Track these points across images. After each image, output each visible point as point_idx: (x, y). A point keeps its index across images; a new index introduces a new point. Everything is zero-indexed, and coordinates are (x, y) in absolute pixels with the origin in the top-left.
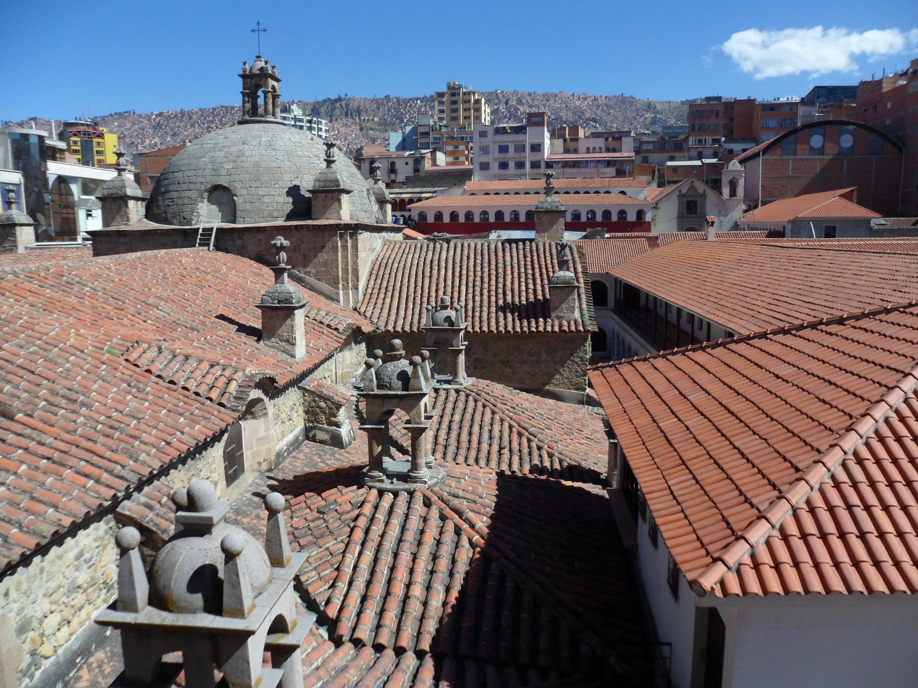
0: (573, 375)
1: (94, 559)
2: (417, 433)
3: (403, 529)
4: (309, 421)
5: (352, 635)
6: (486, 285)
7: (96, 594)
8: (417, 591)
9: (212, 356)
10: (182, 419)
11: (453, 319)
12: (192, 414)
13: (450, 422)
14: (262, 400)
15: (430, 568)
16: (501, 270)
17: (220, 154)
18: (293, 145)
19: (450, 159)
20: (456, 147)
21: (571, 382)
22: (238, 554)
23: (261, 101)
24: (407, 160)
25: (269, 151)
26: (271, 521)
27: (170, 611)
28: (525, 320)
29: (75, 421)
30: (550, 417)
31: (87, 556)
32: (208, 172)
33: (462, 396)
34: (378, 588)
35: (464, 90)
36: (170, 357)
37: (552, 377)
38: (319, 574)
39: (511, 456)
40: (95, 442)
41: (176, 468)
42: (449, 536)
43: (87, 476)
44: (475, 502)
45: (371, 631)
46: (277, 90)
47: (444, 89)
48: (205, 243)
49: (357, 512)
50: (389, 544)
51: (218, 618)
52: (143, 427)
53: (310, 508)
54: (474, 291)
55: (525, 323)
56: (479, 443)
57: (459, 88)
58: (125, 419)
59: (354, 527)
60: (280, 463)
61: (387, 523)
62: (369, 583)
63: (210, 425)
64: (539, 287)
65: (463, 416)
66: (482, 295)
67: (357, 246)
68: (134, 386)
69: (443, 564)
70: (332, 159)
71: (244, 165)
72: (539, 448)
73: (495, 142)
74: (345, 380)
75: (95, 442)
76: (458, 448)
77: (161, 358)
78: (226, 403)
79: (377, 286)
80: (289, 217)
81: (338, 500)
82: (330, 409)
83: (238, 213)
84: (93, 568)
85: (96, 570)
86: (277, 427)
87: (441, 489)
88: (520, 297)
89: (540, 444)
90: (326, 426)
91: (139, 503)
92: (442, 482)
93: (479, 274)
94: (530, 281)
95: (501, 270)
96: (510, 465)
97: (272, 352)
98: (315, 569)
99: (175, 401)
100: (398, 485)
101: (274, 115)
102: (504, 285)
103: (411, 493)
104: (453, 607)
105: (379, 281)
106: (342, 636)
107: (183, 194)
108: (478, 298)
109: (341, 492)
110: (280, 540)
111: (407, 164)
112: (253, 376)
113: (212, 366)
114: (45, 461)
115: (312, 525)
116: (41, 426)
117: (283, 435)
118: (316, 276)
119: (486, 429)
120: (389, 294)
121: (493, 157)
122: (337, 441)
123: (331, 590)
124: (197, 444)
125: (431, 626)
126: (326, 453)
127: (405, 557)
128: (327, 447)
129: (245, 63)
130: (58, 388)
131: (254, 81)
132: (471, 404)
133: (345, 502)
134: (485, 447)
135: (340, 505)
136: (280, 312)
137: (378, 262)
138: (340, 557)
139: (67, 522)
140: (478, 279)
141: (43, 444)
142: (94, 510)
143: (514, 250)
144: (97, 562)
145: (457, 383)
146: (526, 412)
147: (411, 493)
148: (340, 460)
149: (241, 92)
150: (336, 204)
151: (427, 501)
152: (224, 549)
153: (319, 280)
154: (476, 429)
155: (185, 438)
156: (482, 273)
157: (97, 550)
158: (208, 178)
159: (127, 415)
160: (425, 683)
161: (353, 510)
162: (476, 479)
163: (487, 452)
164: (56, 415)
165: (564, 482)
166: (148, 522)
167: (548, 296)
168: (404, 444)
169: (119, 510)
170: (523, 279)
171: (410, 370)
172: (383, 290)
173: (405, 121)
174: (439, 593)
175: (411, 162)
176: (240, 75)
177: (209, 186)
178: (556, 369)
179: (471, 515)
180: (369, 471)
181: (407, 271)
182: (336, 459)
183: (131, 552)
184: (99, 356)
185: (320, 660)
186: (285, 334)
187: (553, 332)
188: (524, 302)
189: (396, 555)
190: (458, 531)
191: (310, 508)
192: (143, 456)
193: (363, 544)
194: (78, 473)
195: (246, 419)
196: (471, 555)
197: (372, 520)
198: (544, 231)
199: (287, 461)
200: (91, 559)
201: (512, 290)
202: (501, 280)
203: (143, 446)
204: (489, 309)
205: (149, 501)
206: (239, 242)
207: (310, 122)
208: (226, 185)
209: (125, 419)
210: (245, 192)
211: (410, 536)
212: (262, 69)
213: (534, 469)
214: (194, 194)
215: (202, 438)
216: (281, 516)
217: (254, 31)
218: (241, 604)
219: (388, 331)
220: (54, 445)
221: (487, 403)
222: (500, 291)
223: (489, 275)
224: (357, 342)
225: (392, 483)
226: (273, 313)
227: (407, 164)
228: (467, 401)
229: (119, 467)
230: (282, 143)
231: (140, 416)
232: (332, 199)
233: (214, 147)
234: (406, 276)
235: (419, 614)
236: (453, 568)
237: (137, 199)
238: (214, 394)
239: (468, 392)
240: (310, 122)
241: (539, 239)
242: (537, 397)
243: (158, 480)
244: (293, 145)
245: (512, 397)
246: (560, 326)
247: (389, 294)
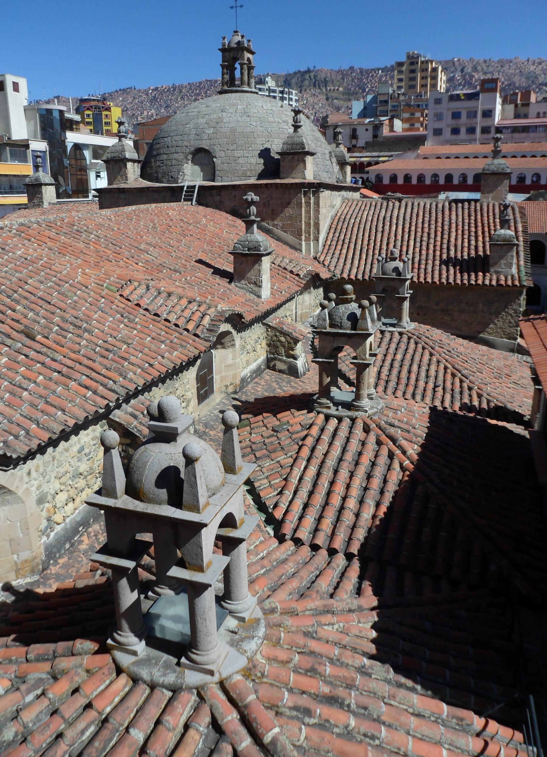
0: (506, 325)
1: (92, 454)
2: (361, 368)
3: (344, 450)
4: (270, 353)
5: (294, 535)
6: (432, 241)
7: (94, 481)
8: (352, 503)
9: (190, 294)
10: (163, 346)
11: (401, 269)
12: (171, 342)
13: (393, 360)
14: (231, 333)
15: (364, 485)
16: (446, 227)
17: (202, 121)
18: (265, 111)
19: (407, 126)
20: (413, 114)
21: (504, 332)
22: (197, 460)
23: (237, 74)
24: (368, 127)
25: (244, 118)
26: (227, 435)
27: (141, 501)
28: (466, 274)
29: (79, 344)
30: (482, 362)
31: (87, 451)
32: (192, 137)
33: (405, 339)
34: (319, 499)
36: (155, 294)
38: (270, 482)
39: (444, 393)
40: (94, 361)
41: (157, 386)
42: (383, 459)
43: (87, 388)
44: (408, 432)
45: (310, 533)
48: (189, 199)
49: (305, 432)
50: (331, 462)
51: (178, 510)
52: (131, 350)
53: (266, 427)
54: (421, 246)
55: (466, 276)
56: (417, 380)
58: (118, 344)
59: (302, 445)
60: (244, 387)
61: (331, 444)
62: (311, 493)
63: (186, 352)
64: (480, 244)
65: (404, 356)
66: (428, 249)
67: (318, 202)
68: (126, 317)
69: (376, 483)
70: (299, 124)
72: (470, 389)
73: (448, 109)
74: (303, 320)
75: (94, 361)
76: (397, 384)
77: (149, 294)
78: (200, 334)
79: (336, 239)
80: (261, 176)
81: (290, 422)
82: (289, 343)
83: (217, 172)
84: (91, 460)
85: (93, 461)
86: (243, 356)
87: (380, 418)
88: (462, 252)
89: (471, 385)
90: (285, 358)
91: (126, 413)
92: (381, 411)
93: (426, 230)
94: (473, 238)
95: (446, 227)
96: (442, 402)
97: (242, 292)
98: (267, 477)
99: (159, 331)
100: (343, 412)
101: (249, 85)
102: (449, 241)
103: (353, 420)
104: (381, 520)
105: (337, 235)
106: (285, 535)
107: (171, 156)
108: (424, 252)
109: (293, 414)
110: (234, 452)
111: (367, 130)
112: (223, 311)
113: (190, 302)
114: (56, 374)
115: (267, 441)
116: (54, 346)
117: (248, 363)
118: (282, 228)
119: (424, 368)
120: (346, 246)
121: (447, 124)
122: (293, 371)
123: (279, 496)
124: (174, 367)
125: (361, 534)
126: (284, 380)
127: (344, 474)
128: (285, 376)
130: (67, 316)
132: (412, 346)
133: (296, 424)
134: (421, 384)
135: (292, 426)
136: (249, 258)
137: (337, 218)
138: (288, 470)
139: (71, 423)
140: (425, 235)
141: (55, 361)
142: (91, 415)
143: (460, 210)
144: (94, 457)
145: (401, 326)
146: (461, 356)
147: (353, 420)
148: (295, 387)
150: (302, 165)
152: (185, 455)
153: (285, 232)
154: (415, 368)
155: (165, 362)
156: (429, 229)
157: (94, 447)
158: (192, 142)
159: (119, 341)
160: (350, 581)
161: (302, 430)
162: (411, 412)
163: (423, 389)
164: (65, 337)
165: (489, 421)
166: (132, 429)
167: (488, 253)
168: (351, 377)
169: (111, 416)
170: (466, 236)
171: (358, 312)
172: (340, 243)
173: (367, 90)
174: (370, 507)
175: (370, 128)
177: (193, 149)
178: (491, 320)
179: (404, 443)
180: (318, 398)
181: (362, 226)
182: (292, 387)
183: (112, 450)
184: (99, 291)
185: (265, 552)
186: (253, 278)
187: (491, 285)
188: (466, 257)
189: (336, 472)
190: (391, 456)
191: (266, 427)
192: (130, 375)
193: (309, 460)
194: (80, 385)
196: (400, 477)
197: (318, 440)
198: (489, 192)
199: (250, 386)
200: (89, 454)
201: (456, 246)
202: (446, 236)
203: (131, 366)
204: (433, 263)
205: (135, 412)
206: (217, 198)
207: (282, 92)
208: (207, 148)
209: (118, 344)
210: (223, 154)
211: (349, 457)
212: (239, 43)
213: (463, 407)
214: (181, 156)
215: (179, 362)
216: (235, 431)
218: (198, 502)
220: (63, 362)
221: (426, 346)
222: (445, 246)
223: (436, 232)
224: (316, 287)
225: (337, 410)
227: (367, 130)
228: (408, 343)
229: (111, 382)
230: (255, 111)
231: (130, 341)
232: (298, 160)
233: (197, 115)
235: (351, 524)
236: (384, 487)
237: (134, 161)
238: (191, 326)
239: (410, 335)
240: (282, 92)
241: (484, 200)
242: (472, 343)
243: (143, 395)
244: (265, 111)
245: (449, 342)
246: (498, 280)
247: (346, 246)
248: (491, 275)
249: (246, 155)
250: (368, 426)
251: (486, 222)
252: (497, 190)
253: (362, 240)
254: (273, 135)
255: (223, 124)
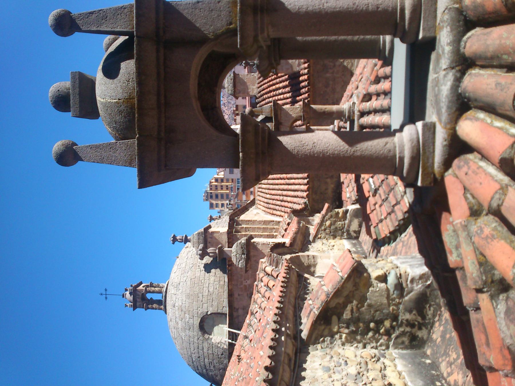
18: (178, 270)
28: (301, 91)
32: (191, 334)
35: (209, 189)
37: (344, 66)
46: (147, 284)
47: (208, 203)
57: (207, 193)
64: (281, 85)
67: (247, 221)
70: (184, 238)
71: (187, 305)
79: (280, 208)
83: (219, 311)
85: (352, 361)
88: (287, 98)
94: (277, 92)
105: (277, 207)
107: (206, 354)
120: (285, 198)
129: (126, 306)
131: (138, 300)
136: (252, 254)
147: (363, 114)
149: (146, 310)
151: (366, 99)
158: (195, 333)
167: (287, 77)
172: (283, 204)
176: (134, 310)
177: (200, 332)
178: (340, 65)
181: (271, 187)
187: (309, 67)
195: (314, 272)
206: (240, 312)
208: (200, 319)
210: (205, 306)
212: (131, 294)
214: (206, 345)
217: (106, 298)
219: (307, 195)
226: (253, 259)
232: (211, 238)
234: (274, 187)
241: (255, 92)
244: (178, 270)
247: (285, 198)
248: (301, 70)
249: (207, 285)
250: (365, 96)
251: (266, 85)
252: (247, 82)
253: (281, 184)
254: (195, 263)
255: (183, 305)
